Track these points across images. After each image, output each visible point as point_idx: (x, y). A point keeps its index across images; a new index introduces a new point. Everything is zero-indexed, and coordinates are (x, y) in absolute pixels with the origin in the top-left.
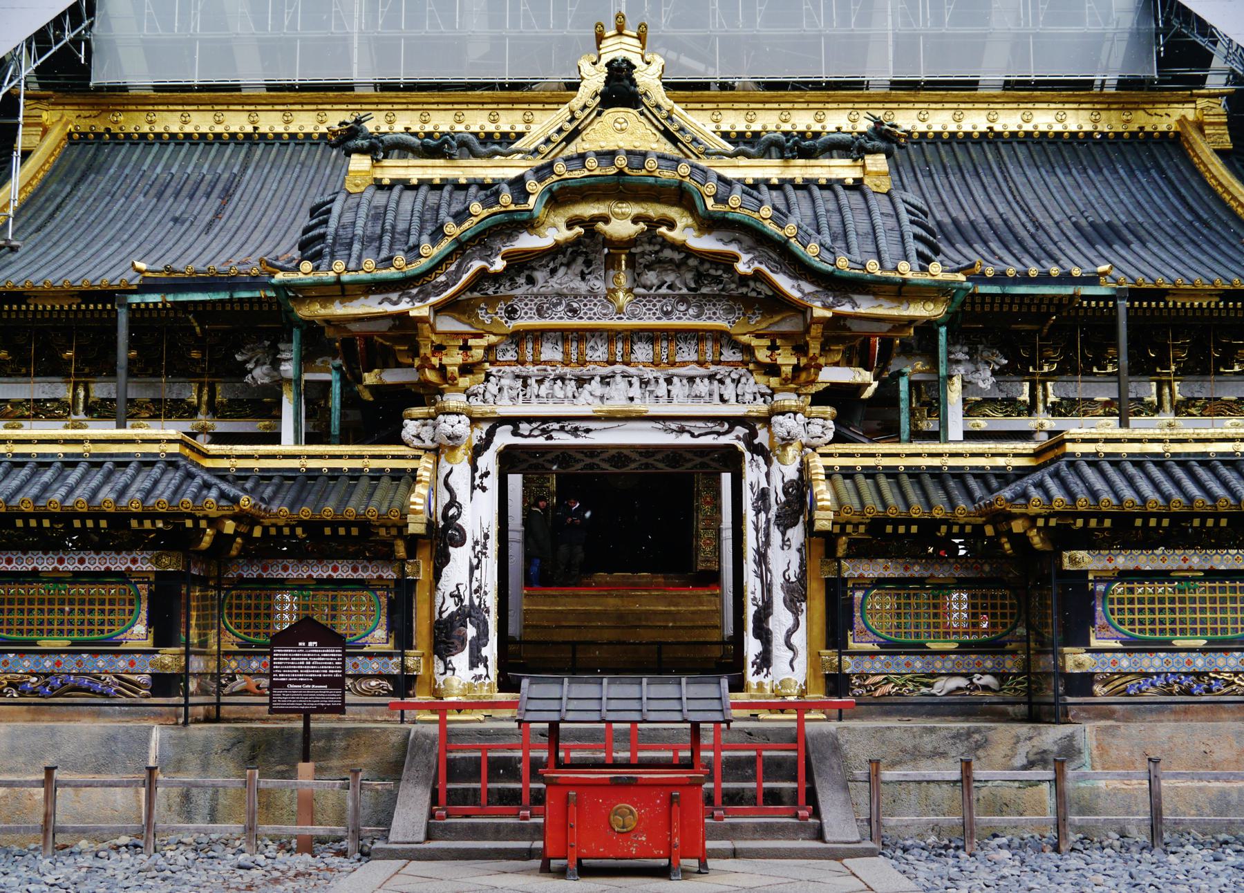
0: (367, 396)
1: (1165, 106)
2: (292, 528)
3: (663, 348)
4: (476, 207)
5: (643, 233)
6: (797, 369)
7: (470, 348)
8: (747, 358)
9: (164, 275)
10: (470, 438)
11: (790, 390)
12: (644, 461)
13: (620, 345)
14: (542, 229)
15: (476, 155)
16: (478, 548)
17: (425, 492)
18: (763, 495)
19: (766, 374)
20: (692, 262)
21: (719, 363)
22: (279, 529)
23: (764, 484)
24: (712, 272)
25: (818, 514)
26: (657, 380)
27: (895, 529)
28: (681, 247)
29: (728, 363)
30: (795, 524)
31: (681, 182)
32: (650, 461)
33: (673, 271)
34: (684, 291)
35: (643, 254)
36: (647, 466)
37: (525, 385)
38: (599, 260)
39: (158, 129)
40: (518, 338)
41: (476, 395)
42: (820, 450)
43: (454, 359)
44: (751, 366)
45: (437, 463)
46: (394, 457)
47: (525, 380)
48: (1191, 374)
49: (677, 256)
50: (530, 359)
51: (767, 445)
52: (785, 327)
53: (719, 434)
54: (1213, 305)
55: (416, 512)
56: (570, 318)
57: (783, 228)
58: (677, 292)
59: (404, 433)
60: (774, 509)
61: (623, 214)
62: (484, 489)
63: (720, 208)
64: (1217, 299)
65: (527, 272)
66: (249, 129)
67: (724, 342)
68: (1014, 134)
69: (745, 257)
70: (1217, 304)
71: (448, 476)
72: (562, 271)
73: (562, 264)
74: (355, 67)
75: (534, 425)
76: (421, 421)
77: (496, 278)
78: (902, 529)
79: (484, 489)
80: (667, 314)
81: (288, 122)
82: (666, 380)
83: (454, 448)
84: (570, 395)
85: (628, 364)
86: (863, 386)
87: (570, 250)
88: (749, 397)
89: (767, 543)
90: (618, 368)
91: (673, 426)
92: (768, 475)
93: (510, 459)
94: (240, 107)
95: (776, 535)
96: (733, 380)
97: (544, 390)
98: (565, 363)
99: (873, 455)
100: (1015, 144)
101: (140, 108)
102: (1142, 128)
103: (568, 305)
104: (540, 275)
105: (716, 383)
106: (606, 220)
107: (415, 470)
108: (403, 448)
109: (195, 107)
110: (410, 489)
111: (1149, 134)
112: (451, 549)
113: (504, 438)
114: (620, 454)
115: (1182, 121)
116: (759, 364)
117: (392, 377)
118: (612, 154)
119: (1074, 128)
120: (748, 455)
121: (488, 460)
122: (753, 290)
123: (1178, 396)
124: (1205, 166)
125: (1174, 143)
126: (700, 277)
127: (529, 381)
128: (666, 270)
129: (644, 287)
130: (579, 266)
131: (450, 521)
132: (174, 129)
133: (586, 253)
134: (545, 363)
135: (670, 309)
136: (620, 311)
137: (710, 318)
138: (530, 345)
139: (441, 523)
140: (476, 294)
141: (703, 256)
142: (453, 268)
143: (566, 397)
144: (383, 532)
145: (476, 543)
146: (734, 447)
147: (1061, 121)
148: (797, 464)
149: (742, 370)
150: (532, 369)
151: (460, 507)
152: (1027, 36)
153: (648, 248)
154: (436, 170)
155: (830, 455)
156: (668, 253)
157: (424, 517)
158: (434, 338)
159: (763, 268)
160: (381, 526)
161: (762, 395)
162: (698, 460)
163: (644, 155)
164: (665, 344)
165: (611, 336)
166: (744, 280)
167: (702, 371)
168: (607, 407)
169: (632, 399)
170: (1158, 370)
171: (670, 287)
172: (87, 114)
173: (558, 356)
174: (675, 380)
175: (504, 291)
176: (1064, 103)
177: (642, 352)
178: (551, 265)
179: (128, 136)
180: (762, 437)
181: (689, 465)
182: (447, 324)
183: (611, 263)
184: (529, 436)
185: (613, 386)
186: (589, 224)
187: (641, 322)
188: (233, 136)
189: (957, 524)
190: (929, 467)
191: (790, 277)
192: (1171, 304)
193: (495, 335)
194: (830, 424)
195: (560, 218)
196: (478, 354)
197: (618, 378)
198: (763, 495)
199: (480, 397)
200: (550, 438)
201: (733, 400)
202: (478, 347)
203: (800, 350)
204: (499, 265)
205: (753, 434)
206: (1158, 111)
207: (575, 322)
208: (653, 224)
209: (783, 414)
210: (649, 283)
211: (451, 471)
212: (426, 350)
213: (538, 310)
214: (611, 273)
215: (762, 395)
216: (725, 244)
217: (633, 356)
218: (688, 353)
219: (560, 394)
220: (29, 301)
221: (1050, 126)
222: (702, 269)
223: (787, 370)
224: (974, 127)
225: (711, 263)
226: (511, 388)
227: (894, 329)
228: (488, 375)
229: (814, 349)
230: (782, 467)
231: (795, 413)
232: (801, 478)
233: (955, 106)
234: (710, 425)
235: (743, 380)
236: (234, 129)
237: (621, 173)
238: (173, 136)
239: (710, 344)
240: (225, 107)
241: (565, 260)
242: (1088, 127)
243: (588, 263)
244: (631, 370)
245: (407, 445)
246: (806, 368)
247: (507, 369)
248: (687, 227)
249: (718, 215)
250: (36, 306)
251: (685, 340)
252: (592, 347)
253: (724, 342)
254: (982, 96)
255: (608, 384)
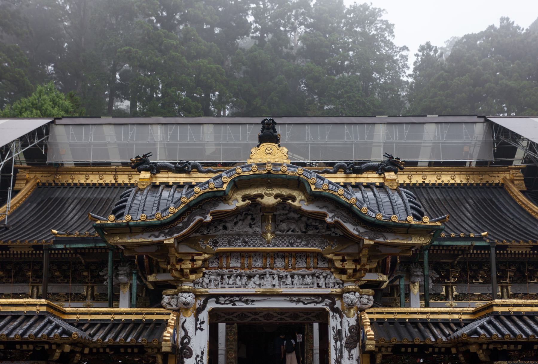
0: (151, 287)
1: (497, 173)
2: (104, 349)
3: (289, 262)
5: (279, 204)
6: (355, 270)
7: (195, 260)
8: (330, 266)
9: (65, 236)
10: (195, 304)
11: (352, 281)
12: (280, 317)
13: (268, 260)
14: (230, 201)
15: (200, 172)
16: (198, 359)
17: (171, 331)
18: (339, 333)
19: (340, 273)
20: (304, 219)
21: (317, 268)
22: (98, 349)
23: (339, 327)
24: (314, 224)
25: (368, 342)
26: (286, 276)
27: (406, 350)
28: (298, 210)
29: (321, 268)
30: (355, 347)
31: (299, 177)
32: (283, 317)
33: (295, 223)
34: (300, 233)
35: (280, 215)
36: (281, 319)
37: (222, 278)
38: (258, 217)
39: (76, 181)
40: (219, 256)
41: (198, 283)
42: (367, 311)
43: (187, 265)
44: (332, 270)
45: (178, 317)
46: (158, 314)
47: (222, 276)
48: (516, 283)
49: (296, 216)
50: (225, 266)
51: (340, 308)
52: (349, 251)
53: (317, 303)
54: (528, 252)
55: (166, 341)
56: (244, 246)
57: (349, 200)
58: (296, 233)
59: (162, 302)
60: (344, 340)
61: (270, 194)
62: (202, 330)
63: (317, 190)
64: (530, 250)
65: (223, 224)
66: (114, 182)
67: (319, 258)
68: (434, 184)
69: (330, 215)
70: (529, 252)
71: (184, 323)
72: (240, 223)
73: (240, 220)
74: (158, 156)
75: (227, 298)
76: (171, 296)
77: (208, 225)
78: (409, 350)
79: (202, 330)
80: (292, 244)
81: (130, 179)
82: (291, 276)
83: (187, 309)
84: (244, 283)
85: (272, 269)
86: (384, 282)
87: (244, 213)
88: (331, 285)
89: (341, 357)
90: (268, 270)
91: (295, 299)
92: (341, 323)
93: (215, 315)
94: (110, 173)
95: (346, 353)
96: (324, 277)
97: (231, 281)
98: (242, 268)
99: (393, 313)
100: (434, 188)
101: (68, 173)
102: (487, 182)
103: (243, 239)
104: (229, 225)
105: (315, 278)
106: (261, 196)
107: (167, 320)
108: (162, 309)
109: (91, 173)
110: (164, 329)
111: (491, 184)
112: (185, 359)
113: (212, 305)
114: (268, 313)
115: (505, 179)
116: (336, 268)
117: (162, 277)
119: (459, 182)
120: (331, 313)
121: (204, 316)
122: (334, 232)
123: (510, 293)
124: (516, 196)
125: (501, 187)
127: (224, 277)
128: (291, 223)
129: (280, 231)
130: (249, 220)
131: (185, 346)
132: (82, 181)
133: (252, 215)
134: (232, 268)
135: (293, 241)
136: (268, 243)
137: (312, 246)
138: (225, 260)
139: (180, 346)
140: (198, 234)
142: (186, 220)
143: (242, 284)
144: (150, 351)
145: (198, 356)
146: (324, 309)
147: (453, 179)
148: (355, 317)
149: (329, 272)
150: (226, 271)
151: (189, 339)
152: (439, 143)
153: (282, 212)
154: (182, 179)
155: (372, 313)
156: (292, 215)
157: (169, 343)
158: (177, 255)
159: (339, 220)
160: (149, 348)
161: (338, 284)
162: (306, 317)
164: (290, 259)
165: (264, 255)
166: (329, 226)
167: (308, 272)
168: (262, 289)
169: (274, 286)
170: (501, 281)
171: (293, 231)
172: (45, 175)
173: (239, 265)
174: (296, 276)
175: (212, 233)
176: (454, 171)
177: (279, 263)
178: (235, 220)
179: (63, 184)
180: (338, 304)
181: (301, 319)
182: (184, 249)
183: (264, 220)
184: (224, 304)
185: (265, 279)
186: (253, 198)
187: (279, 248)
188: (107, 184)
189: (437, 347)
190: (420, 319)
191: (353, 224)
192: (509, 252)
193: (207, 254)
194: (371, 298)
195: (239, 196)
196: (199, 263)
197: (268, 276)
198: (339, 333)
199: (200, 285)
200: (234, 305)
201: (324, 286)
202: (199, 260)
203: (357, 261)
204: (209, 218)
205: (334, 303)
206: (494, 175)
207: (247, 248)
208: (285, 198)
209: (349, 292)
210: (283, 229)
211: (185, 321)
212: (173, 260)
213: (228, 242)
214: (264, 224)
215: (338, 284)
216: (320, 208)
217: (275, 265)
219: (239, 283)
220: (10, 250)
221: (449, 181)
222: (308, 222)
223: (350, 271)
224: (417, 181)
225: (313, 219)
226: (215, 280)
227: (403, 251)
228: (204, 274)
229: (364, 260)
230: (349, 319)
231: (355, 292)
232: (358, 324)
233: (409, 173)
234: (313, 298)
235: (329, 276)
236: (108, 181)
237: (269, 172)
238: (82, 184)
239: (312, 259)
240: (104, 173)
241: (242, 218)
242: (464, 182)
243: (253, 219)
244: (274, 271)
245: (164, 308)
246: (360, 270)
247: (214, 271)
248: (301, 200)
249: (317, 193)
250: (13, 252)
251: (300, 257)
252: (255, 261)
253: (319, 258)
254: (419, 169)
255: (263, 278)
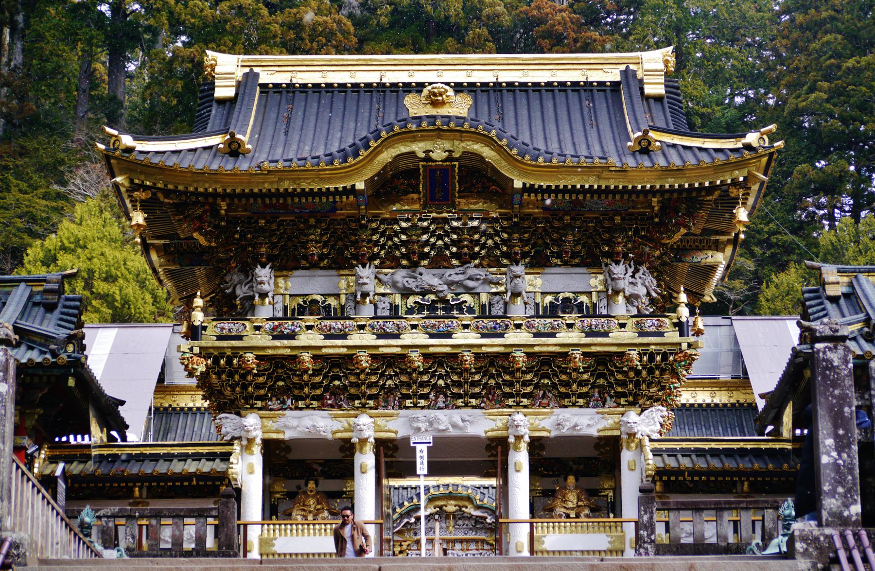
4: (406, 503)
5: (457, 511)
69: (489, 517)
118: (448, 485)
126: (476, 522)
141: (477, 517)
156: (465, 515)
163: (458, 486)
177: (458, 546)
179: (182, 409)
186: (441, 507)
196: (405, 547)
218: (473, 546)
